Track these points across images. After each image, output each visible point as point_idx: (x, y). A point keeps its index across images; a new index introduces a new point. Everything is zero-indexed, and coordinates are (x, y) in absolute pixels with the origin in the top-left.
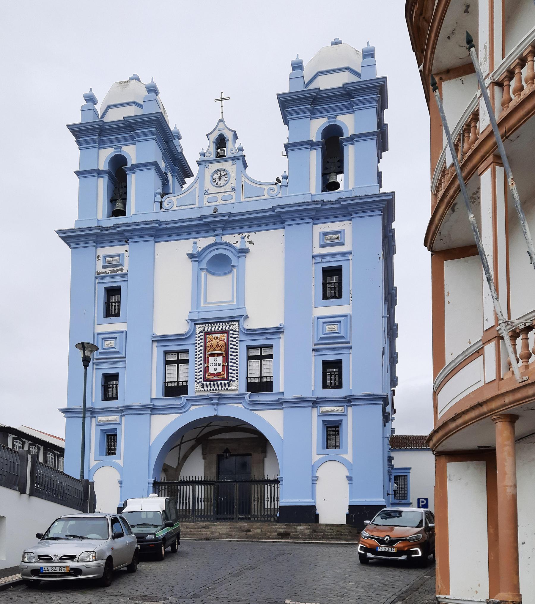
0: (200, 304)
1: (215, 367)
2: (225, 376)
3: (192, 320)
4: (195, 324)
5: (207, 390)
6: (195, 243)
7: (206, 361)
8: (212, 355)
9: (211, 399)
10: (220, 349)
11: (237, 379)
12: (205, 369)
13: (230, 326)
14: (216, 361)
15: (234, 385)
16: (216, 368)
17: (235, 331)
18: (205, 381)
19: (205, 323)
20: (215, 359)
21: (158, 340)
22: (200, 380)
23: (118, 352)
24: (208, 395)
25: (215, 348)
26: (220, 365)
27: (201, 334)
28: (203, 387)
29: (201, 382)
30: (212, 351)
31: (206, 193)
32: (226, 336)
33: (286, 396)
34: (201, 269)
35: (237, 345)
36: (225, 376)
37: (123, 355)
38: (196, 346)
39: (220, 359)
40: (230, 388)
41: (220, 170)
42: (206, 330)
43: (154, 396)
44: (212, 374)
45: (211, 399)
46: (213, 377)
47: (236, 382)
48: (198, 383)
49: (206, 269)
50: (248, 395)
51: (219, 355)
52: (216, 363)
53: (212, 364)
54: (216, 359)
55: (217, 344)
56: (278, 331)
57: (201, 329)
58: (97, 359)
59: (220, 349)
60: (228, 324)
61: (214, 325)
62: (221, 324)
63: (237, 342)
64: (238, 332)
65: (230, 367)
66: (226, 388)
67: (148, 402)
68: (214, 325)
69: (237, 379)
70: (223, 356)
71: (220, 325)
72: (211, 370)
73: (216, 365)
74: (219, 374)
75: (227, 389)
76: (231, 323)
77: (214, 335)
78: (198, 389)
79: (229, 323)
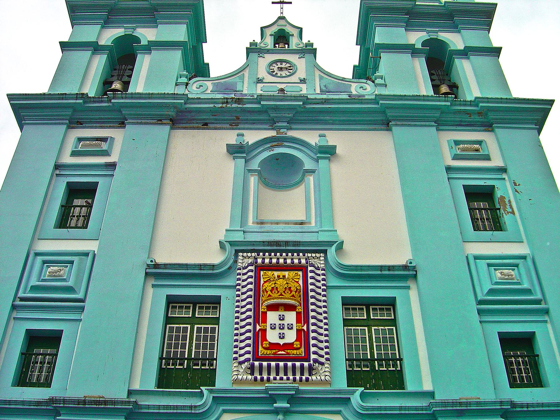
0: (247, 221)
1: (282, 331)
2: (301, 352)
3: (232, 243)
4: (237, 252)
5: (262, 379)
8: (274, 307)
9: (272, 399)
10: (293, 296)
11: (327, 359)
12: (256, 334)
13: (306, 259)
14: (283, 319)
15: (322, 373)
16: (283, 333)
17: (318, 269)
18: (256, 357)
19: (258, 252)
20: (280, 315)
22: (247, 356)
23: (70, 289)
24: (266, 391)
25: (283, 294)
26: (292, 328)
27: (250, 268)
28: (252, 374)
29: (248, 360)
30: (275, 298)
32: (301, 275)
34: (250, 171)
35: (323, 293)
36: (301, 352)
37: (80, 296)
38: (239, 290)
39: (291, 317)
40: (314, 378)
41: (281, 61)
42: (260, 261)
44: (273, 346)
45: (272, 399)
46: (274, 351)
47: (326, 366)
48: (241, 363)
49: (260, 173)
50: (358, 394)
51: (289, 308)
52: (283, 324)
53: (275, 324)
54: (283, 315)
55: (286, 286)
57: (250, 261)
58: (22, 299)
59: (293, 296)
60: (304, 255)
61: (275, 255)
62: (290, 254)
63: (322, 287)
64: (323, 270)
65: (312, 335)
66: (304, 378)
67: (123, 396)
68: (275, 255)
69: (327, 359)
70: (297, 310)
71: (287, 255)
72: (272, 337)
73: (282, 327)
75: (307, 379)
76: (309, 255)
77: (276, 273)
78: (240, 377)
79: (306, 254)
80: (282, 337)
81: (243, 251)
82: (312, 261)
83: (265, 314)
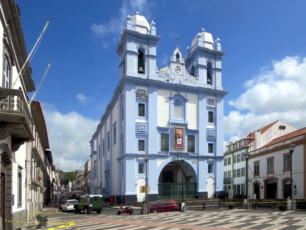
4: (172, 124)
6: (171, 93)
7: (176, 139)
8: (178, 137)
21: (159, 129)
31: (174, 74)
33: (200, 155)
34: (173, 103)
39: (181, 139)
43: (158, 151)
44: (178, 145)
51: (180, 137)
56: (197, 132)
72: (178, 143)
74: (180, 145)
77: (178, 130)
80: (179, 143)
81: (173, 124)
82: (184, 128)
83: (177, 138)
